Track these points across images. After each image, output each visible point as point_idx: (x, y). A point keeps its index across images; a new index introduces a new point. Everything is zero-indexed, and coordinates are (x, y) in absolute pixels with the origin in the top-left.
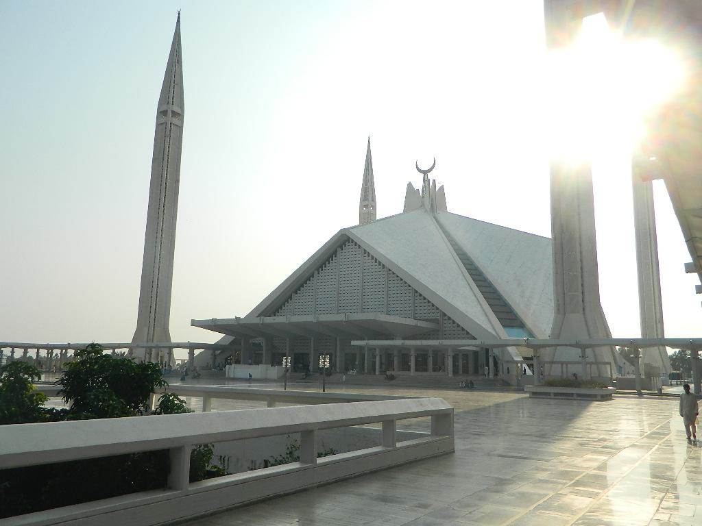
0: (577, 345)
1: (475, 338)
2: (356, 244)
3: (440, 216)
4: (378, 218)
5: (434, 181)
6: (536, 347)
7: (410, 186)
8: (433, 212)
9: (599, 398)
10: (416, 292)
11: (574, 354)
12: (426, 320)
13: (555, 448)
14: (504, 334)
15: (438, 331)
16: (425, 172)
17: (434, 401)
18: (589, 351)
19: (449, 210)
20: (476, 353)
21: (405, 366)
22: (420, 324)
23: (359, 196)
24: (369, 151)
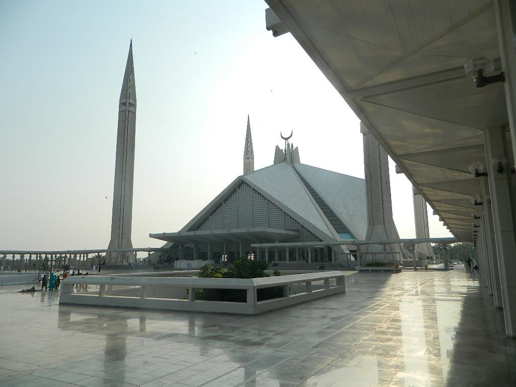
0: (381, 243)
1: (321, 241)
2: (248, 185)
3: (296, 166)
4: (256, 168)
5: (292, 144)
6: (359, 245)
7: (277, 147)
8: (292, 164)
9: (395, 272)
10: (285, 213)
11: (380, 248)
12: (293, 230)
13: (383, 289)
14: (339, 238)
15: (299, 236)
16: (286, 139)
17: (338, 273)
18: (387, 246)
19: (302, 162)
20: (322, 249)
21: (281, 258)
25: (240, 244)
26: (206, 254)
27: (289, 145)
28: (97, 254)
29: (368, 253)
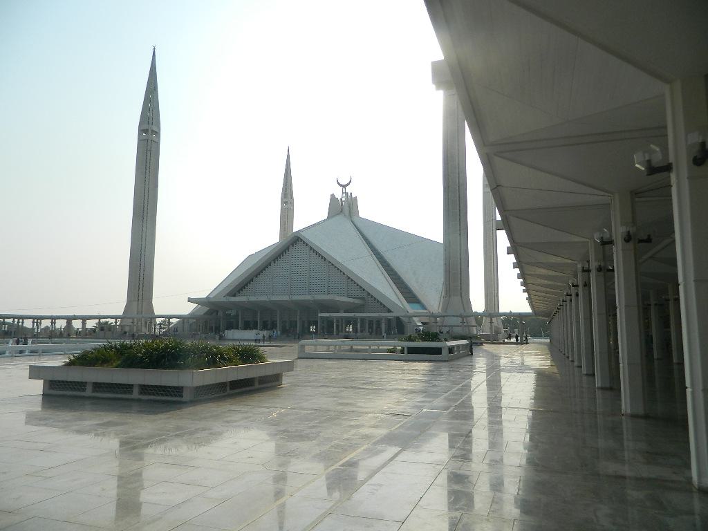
1: (389, 311)
2: (304, 242)
3: (355, 220)
5: (351, 194)
7: (333, 196)
10: (349, 278)
11: (458, 321)
12: (358, 298)
14: (411, 309)
15: (363, 305)
16: (344, 186)
19: (362, 214)
20: (390, 320)
22: (357, 301)
23: (280, 196)
24: (288, 156)
25: (278, 312)
26: (256, 323)
27: (347, 194)
28: (97, 321)
29: (446, 326)
